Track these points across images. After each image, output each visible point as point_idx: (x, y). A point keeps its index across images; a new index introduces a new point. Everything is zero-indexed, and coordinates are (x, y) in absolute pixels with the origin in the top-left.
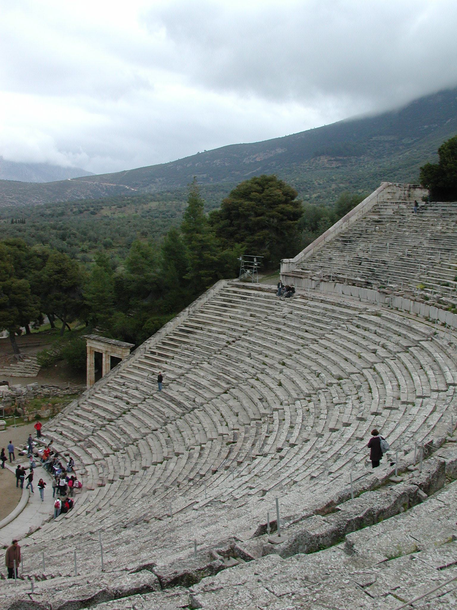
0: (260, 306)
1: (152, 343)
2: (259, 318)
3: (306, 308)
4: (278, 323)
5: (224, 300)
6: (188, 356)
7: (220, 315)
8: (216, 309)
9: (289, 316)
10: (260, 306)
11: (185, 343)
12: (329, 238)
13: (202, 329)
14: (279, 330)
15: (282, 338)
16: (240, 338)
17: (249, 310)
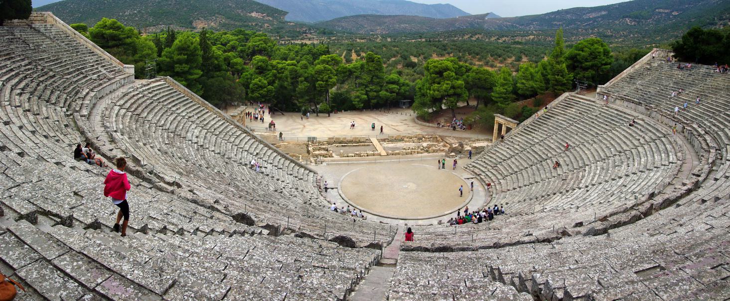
0: (585, 109)
1: (528, 122)
2: (584, 115)
3: (608, 112)
4: (593, 119)
5: (567, 103)
6: (546, 131)
7: (564, 111)
8: (562, 108)
9: (599, 116)
10: (585, 109)
11: (545, 124)
12: (623, 76)
13: (554, 117)
14: (593, 122)
15: (594, 127)
16: (572, 125)
17: (579, 110)
